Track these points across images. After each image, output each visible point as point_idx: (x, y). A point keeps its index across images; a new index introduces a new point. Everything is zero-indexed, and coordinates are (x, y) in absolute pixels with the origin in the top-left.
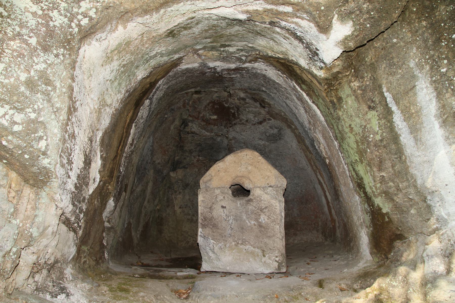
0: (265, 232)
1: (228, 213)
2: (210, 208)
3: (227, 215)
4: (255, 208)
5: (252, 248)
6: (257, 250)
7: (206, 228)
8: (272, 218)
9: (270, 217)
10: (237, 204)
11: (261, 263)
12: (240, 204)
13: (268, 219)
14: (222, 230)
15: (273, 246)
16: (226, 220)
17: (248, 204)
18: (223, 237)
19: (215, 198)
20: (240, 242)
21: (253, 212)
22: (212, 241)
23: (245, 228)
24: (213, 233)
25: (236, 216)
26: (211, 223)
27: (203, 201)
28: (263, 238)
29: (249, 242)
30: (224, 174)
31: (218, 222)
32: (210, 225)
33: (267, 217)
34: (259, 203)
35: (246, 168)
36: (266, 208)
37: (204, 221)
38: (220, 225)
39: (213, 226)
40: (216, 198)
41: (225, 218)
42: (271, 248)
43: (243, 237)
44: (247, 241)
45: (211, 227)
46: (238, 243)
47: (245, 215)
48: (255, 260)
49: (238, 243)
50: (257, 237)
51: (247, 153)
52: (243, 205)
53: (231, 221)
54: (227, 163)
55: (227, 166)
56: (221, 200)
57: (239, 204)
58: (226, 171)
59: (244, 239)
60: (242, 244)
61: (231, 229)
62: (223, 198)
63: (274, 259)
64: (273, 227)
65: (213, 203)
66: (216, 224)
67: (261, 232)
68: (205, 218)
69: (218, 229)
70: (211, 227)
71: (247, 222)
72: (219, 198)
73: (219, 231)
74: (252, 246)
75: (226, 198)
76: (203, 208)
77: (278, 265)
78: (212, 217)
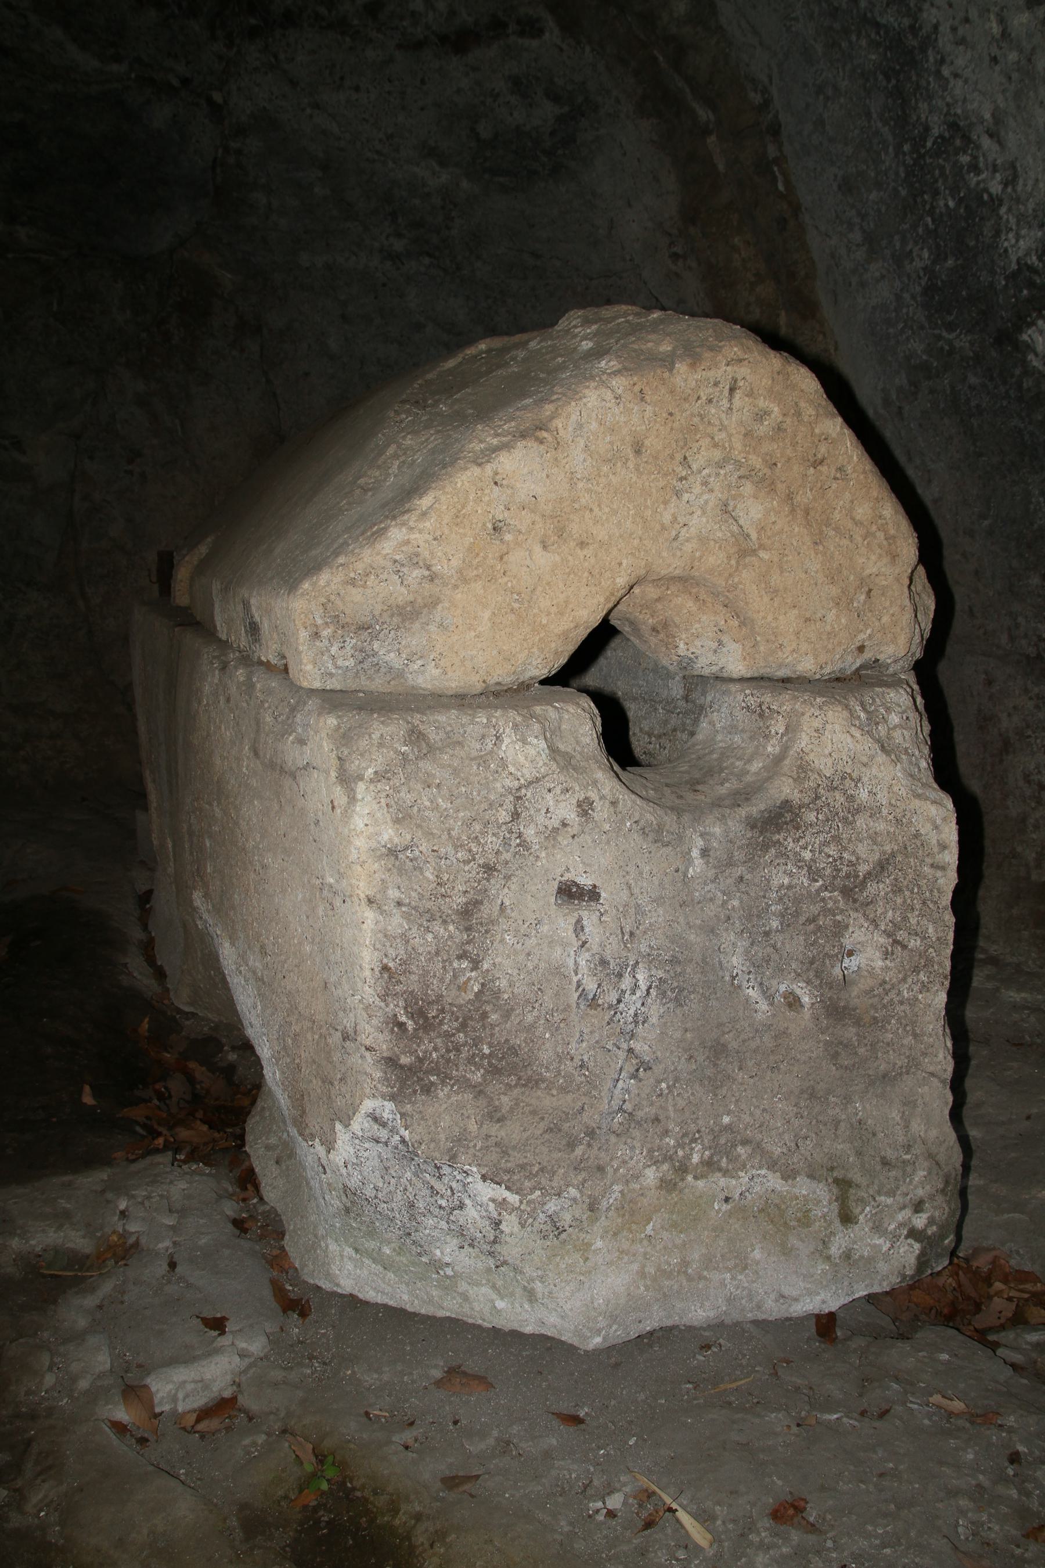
0: (862, 1051)
1: (613, 949)
2: (466, 912)
3: (604, 962)
4: (814, 874)
5: (774, 1181)
6: (803, 1187)
7: (428, 1089)
8: (914, 943)
9: (901, 935)
10: (686, 856)
11: (822, 1267)
12: (705, 853)
13: (886, 955)
14: (564, 1090)
15: (901, 1139)
16: (593, 1003)
17: (765, 847)
18: (571, 1145)
19: (503, 816)
20: (696, 1159)
21: (797, 914)
22: (486, 1191)
23: (734, 1045)
24: (494, 1129)
25: (674, 961)
26: (477, 1042)
27: (393, 852)
28: (848, 1099)
29: (759, 1145)
30: (543, 559)
31: (533, 1026)
32: (470, 1060)
33: (882, 940)
34: (837, 839)
35: (725, 509)
36: (882, 866)
37: (415, 1036)
38: (546, 1054)
39: (495, 1071)
40: (516, 815)
41: (591, 986)
42: (890, 1154)
43: (718, 1116)
44: (745, 1142)
45: (477, 1077)
46: (683, 1169)
47: (742, 944)
48: (787, 1252)
49: (683, 1169)
50: (812, 1095)
51: (743, 371)
52: (730, 863)
53: (632, 1004)
54: (577, 458)
55: (572, 481)
56: (552, 835)
57: (695, 853)
58: (561, 532)
59: (729, 1128)
60: (710, 1165)
61: (630, 1068)
62: (571, 815)
63: (901, 1225)
64: (913, 1002)
65: (489, 869)
66: (514, 1051)
67: (835, 1056)
68: (419, 1014)
69: (534, 1082)
70: (477, 1077)
71: (753, 993)
72: (541, 819)
73: (547, 1101)
74: (772, 1166)
75: (601, 812)
76: (397, 922)
77: (920, 1257)
78: (488, 993)
